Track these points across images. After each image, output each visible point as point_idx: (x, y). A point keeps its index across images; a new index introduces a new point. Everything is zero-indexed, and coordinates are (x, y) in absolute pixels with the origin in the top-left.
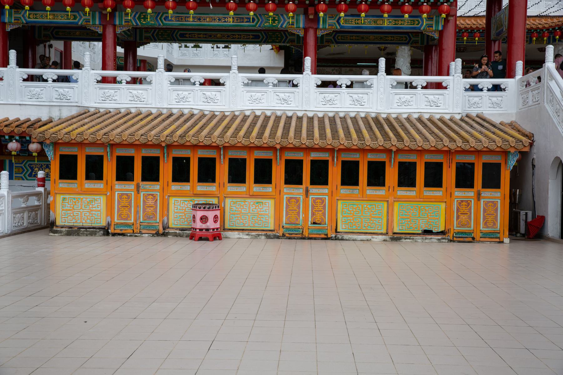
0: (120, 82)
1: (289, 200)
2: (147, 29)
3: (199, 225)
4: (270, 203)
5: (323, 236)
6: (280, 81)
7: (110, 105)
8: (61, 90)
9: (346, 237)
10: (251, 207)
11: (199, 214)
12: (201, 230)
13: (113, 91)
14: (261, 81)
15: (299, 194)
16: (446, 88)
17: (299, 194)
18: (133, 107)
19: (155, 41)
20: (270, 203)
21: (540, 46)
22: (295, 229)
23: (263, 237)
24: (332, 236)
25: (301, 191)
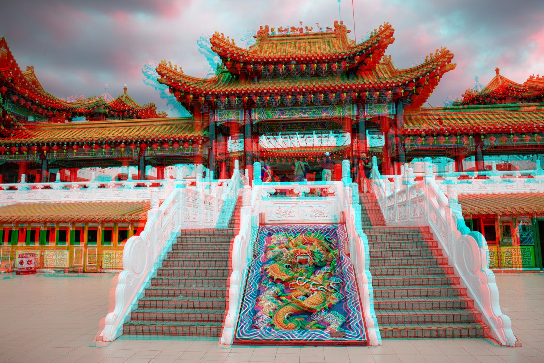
0: (38, 189)
1: (77, 251)
2: (81, 160)
3: (25, 265)
4: (67, 253)
5: (94, 271)
6: (116, 185)
7: (32, 201)
8: (9, 194)
9: (106, 271)
10: (56, 255)
11: (25, 260)
12: (27, 268)
13: (33, 193)
14: (121, 185)
15: (82, 247)
16: (162, 186)
17: (82, 247)
19: (85, 167)
20: (67, 253)
21: (292, 162)
22: (78, 266)
23: (62, 272)
24: (99, 270)
25: (83, 245)
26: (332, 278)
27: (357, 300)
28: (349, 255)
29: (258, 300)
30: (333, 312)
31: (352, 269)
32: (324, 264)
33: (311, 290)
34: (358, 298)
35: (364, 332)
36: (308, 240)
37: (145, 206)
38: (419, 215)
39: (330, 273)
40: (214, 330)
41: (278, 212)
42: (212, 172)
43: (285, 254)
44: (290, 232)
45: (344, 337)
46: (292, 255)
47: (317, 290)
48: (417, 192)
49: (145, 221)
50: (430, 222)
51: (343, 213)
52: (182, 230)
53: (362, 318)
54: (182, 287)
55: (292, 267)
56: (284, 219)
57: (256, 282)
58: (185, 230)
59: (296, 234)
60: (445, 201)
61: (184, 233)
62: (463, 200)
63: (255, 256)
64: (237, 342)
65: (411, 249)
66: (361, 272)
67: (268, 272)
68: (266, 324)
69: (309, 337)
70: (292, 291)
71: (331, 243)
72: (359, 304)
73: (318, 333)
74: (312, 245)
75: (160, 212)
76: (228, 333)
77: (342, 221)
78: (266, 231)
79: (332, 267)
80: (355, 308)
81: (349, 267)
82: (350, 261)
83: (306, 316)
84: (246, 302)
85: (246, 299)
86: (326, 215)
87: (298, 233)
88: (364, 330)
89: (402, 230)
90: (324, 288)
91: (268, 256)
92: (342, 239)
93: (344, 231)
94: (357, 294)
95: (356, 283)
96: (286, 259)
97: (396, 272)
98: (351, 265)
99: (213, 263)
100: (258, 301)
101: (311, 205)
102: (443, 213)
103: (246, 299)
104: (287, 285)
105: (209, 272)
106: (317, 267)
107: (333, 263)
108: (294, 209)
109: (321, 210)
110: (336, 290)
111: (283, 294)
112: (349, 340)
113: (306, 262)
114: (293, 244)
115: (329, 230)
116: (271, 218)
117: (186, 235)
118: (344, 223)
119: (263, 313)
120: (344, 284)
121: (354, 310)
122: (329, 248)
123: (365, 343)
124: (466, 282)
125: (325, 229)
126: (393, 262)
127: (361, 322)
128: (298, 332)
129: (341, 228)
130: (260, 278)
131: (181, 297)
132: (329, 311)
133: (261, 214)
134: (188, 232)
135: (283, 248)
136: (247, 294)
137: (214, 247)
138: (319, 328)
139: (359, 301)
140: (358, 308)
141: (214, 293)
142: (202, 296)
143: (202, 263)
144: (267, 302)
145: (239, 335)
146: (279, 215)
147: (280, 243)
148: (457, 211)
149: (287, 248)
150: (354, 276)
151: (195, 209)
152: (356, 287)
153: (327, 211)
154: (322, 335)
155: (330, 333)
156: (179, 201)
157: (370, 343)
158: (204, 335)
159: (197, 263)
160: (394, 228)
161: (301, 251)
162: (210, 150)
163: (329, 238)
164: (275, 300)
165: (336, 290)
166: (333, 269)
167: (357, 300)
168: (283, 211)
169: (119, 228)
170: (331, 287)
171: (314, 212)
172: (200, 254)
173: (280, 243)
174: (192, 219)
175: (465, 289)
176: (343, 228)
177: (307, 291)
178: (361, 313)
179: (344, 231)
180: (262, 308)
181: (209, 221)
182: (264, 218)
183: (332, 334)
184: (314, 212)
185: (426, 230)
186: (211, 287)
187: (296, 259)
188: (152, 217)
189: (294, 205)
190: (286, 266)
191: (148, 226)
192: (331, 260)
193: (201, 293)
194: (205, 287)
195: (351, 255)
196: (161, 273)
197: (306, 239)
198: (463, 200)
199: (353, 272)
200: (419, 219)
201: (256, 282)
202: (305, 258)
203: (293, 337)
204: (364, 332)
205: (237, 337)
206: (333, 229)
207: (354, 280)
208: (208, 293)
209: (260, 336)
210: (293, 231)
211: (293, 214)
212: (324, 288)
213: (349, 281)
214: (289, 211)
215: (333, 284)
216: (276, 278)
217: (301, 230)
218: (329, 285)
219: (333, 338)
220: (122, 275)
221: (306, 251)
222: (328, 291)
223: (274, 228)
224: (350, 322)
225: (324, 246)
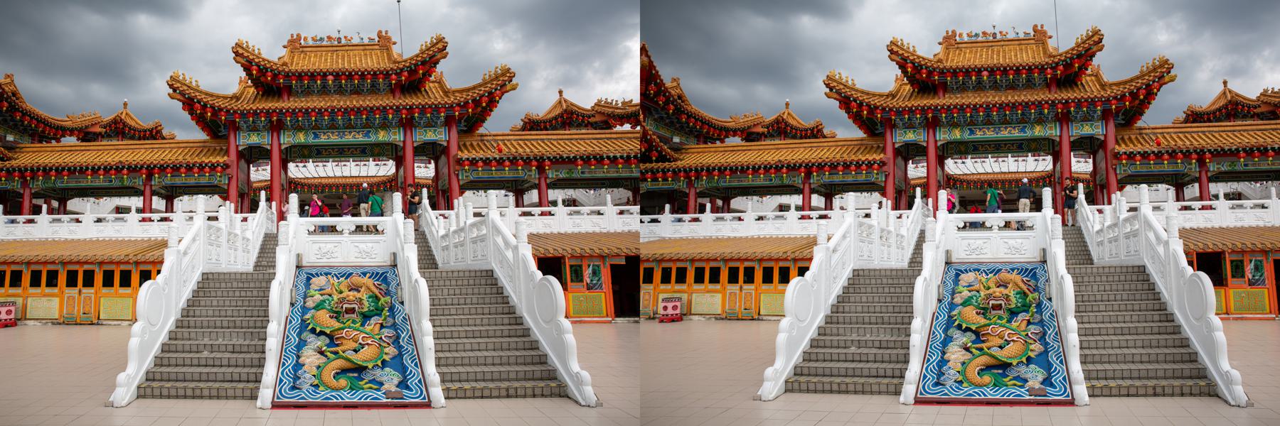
18: (24, 237)
31: (407, 319)
37: (164, 244)
49: (162, 262)
54: (206, 341)
60: (513, 241)
62: (533, 238)
65: (475, 295)
75: (179, 251)
78: (305, 274)
97: (458, 323)
99: (242, 313)
102: (509, 254)
104: (332, 339)
105: (238, 324)
113: (352, 311)
120: (398, 337)
124: (537, 334)
126: (453, 312)
137: (243, 294)
141: (245, 349)
148: (527, 252)
156: (200, 239)
159: (223, 313)
169: (131, 271)
172: (228, 304)
175: (537, 342)
186: (241, 342)
188: (170, 258)
191: (165, 268)
194: (234, 341)
195: (406, 303)
196: (179, 324)
198: (533, 238)
208: (237, 349)
216: (318, 330)
220: (137, 327)
223: (314, 272)
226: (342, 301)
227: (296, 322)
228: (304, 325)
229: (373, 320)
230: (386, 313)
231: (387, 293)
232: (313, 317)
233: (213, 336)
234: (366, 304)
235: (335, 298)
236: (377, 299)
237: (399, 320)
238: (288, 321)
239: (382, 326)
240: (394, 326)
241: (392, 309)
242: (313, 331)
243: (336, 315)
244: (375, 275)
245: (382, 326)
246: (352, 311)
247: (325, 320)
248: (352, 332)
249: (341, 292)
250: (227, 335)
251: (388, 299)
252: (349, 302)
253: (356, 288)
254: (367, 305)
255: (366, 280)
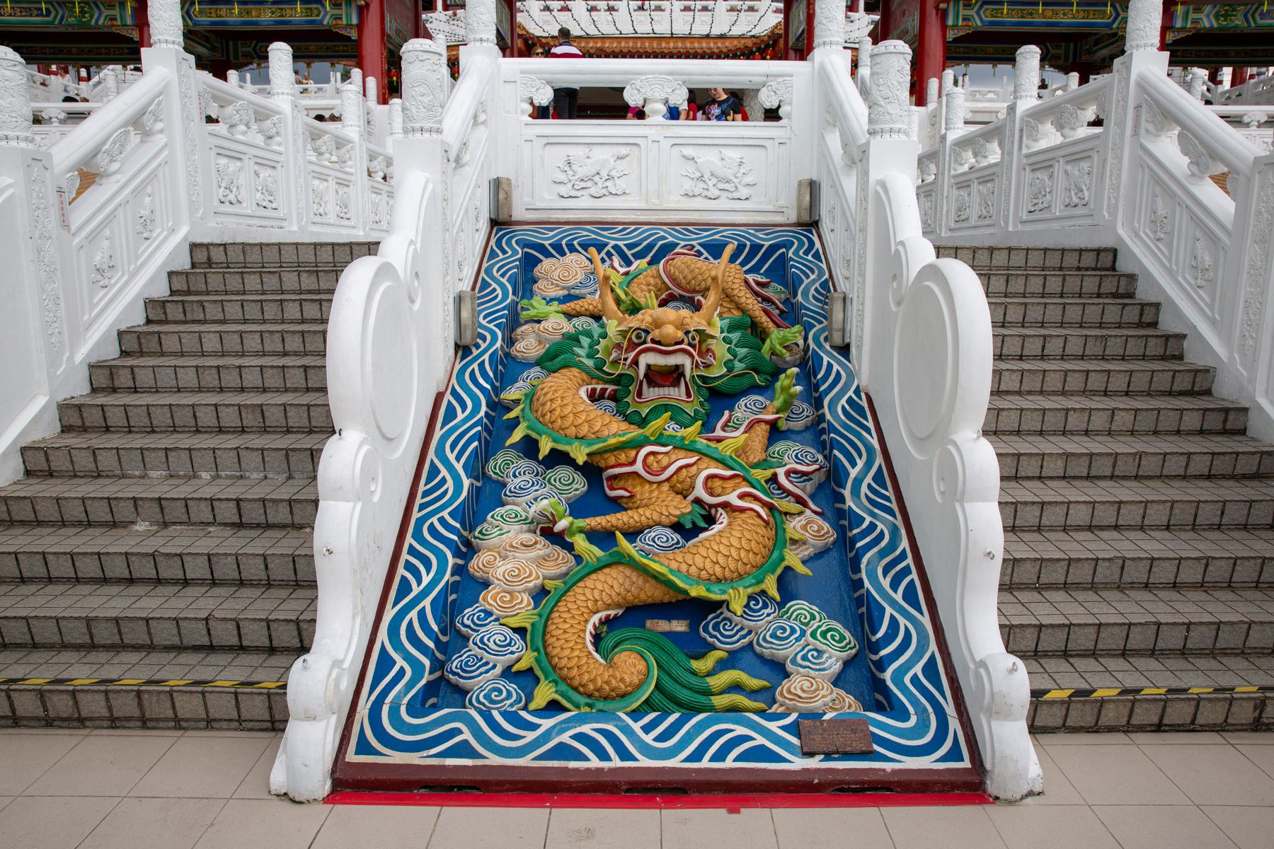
26: (780, 446)
27: (903, 556)
28: (844, 350)
29: (468, 543)
30: (800, 606)
31: (864, 409)
32: (746, 382)
33: (698, 501)
34: (905, 544)
35: (954, 724)
36: (679, 286)
38: (1057, 211)
39: (773, 425)
40: (255, 708)
41: (562, 177)
42: (372, 82)
43: (585, 341)
44: (609, 254)
45: (868, 755)
46: (618, 346)
47: (726, 505)
48: (975, 155)
50: (1121, 231)
51: (813, 187)
52: (194, 247)
53: (933, 647)
55: (613, 397)
56: (584, 206)
57: (459, 467)
58: (207, 246)
59: (629, 263)
61: (201, 256)
63: (462, 349)
64: (352, 785)
66: (936, 435)
67: (515, 422)
68: (498, 670)
69: (697, 756)
70: (617, 505)
71: (766, 299)
72: (914, 575)
73: (740, 730)
74: (697, 307)
76: (310, 746)
77: (806, 218)
79: (778, 402)
80: (898, 597)
81: (850, 401)
82: (851, 376)
83: (679, 626)
84: (409, 567)
85: (412, 551)
86: (744, 192)
87: (638, 256)
88: (950, 709)
89: (1017, 259)
90: (756, 499)
91: (519, 346)
92: (810, 283)
93: (816, 256)
94: (899, 522)
95: (888, 476)
96: (590, 363)
98: (857, 392)
100: (467, 550)
101: (689, 151)
103: (412, 551)
106: (719, 397)
107: (783, 381)
108: (621, 165)
109: (729, 174)
110: (799, 500)
111: (581, 523)
112: (888, 766)
113: (673, 376)
114: (618, 301)
115: (756, 248)
116: (537, 198)
117: (210, 263)
118: (810, 224)
119: (488, 614)
121: (894, 604)
122: (764, 319)
123: (968, 786)
125: (741, 247)
127: (930, 670)
128: (647, 729)
129: (801, 244)
130: (487, 433)
131: (141, 527)
132: (781, 605)
133: (497, 185)
134: (218, 256)
135: (578, 315)
136: (420, 522)
138: (736, 687)
139: (909, 560)
140: (910, 595)
142: (233, 525)
143: (252, 378)
144: (512, 559)
145: (364, 747)
146: (564, 190)
147: (569, 298)
149: (597, 318)
150: (875, 442)
151: (265, 173)
152: (890, 493)
153: (748, 180)
154: (760, 740)
155: (794, 729)
157: (992, 788)
158: (210, 723)
160: (992, 250)
161: (656, 334)
162: (362, 11)
163: (759, 279)
164: (544, 548)
165: (799, 500)
166: (787, 406)
167: (903, 556)
168: (582, 172)
170: (780, 487)
171: (701, 178)
173: (569, 298)
174: (247, 208)
176: (812, 243)
177: (680, 508)
178: (926, 620)
179: (816, 256)
180: (486, 584)
181: (332, 218)
182: (508, 197)
183: (806, 727)
184: (701, 178)
185: (1106, 260)
187: (635, 362)
189: (623, 151)
190: (594, 397)
192: (769, 369)
193: (227, 512)
197: (673, 280)
199: (870, 424)
200: (1056, 225)
201: (459, 467)
202: (672, 361)
203: (625, 754)
204: (954, 724)
205: (351, 757)
206: (773, 248)
207: (879, 460)
209: (463, 749)
210: (616, 247)
211: (621, 184)
212: (756, 499)
213: (860, 464)
214: (604, 174)
215: (788, 474)
216: (545, 447)
217: (650, 247)
218: (774, 479)
219: (814, 763)
221: (680, 334)
222: (771, 508)
224: (881, 665)
225: (743, 311)
226: (637, 340)
227: (471, 416)
228: (498, 420)
229: (744, 409)
230: (789, 382)
231: (789, 314)
232: (531, 397)
233: (180, 463)
234: (720, 350)
235: (612, 327)
236: (757, 332)
237: (835, 411)
238: (439, 411)
239: (775, 432)
240: (818, 433)
241: (808, 366)
242: (529, 447)
243: (615, 391)
244: (748, 253)
245: (775, 432)
246: (673, 376)
247: (570, 407)
248: (672, 460)
249: (634, 309)
250: (227, 459)
251: (794, 334)
252: (660, 345)
253: (684, 295)
254: (723, 357)
255: (720, 267)
